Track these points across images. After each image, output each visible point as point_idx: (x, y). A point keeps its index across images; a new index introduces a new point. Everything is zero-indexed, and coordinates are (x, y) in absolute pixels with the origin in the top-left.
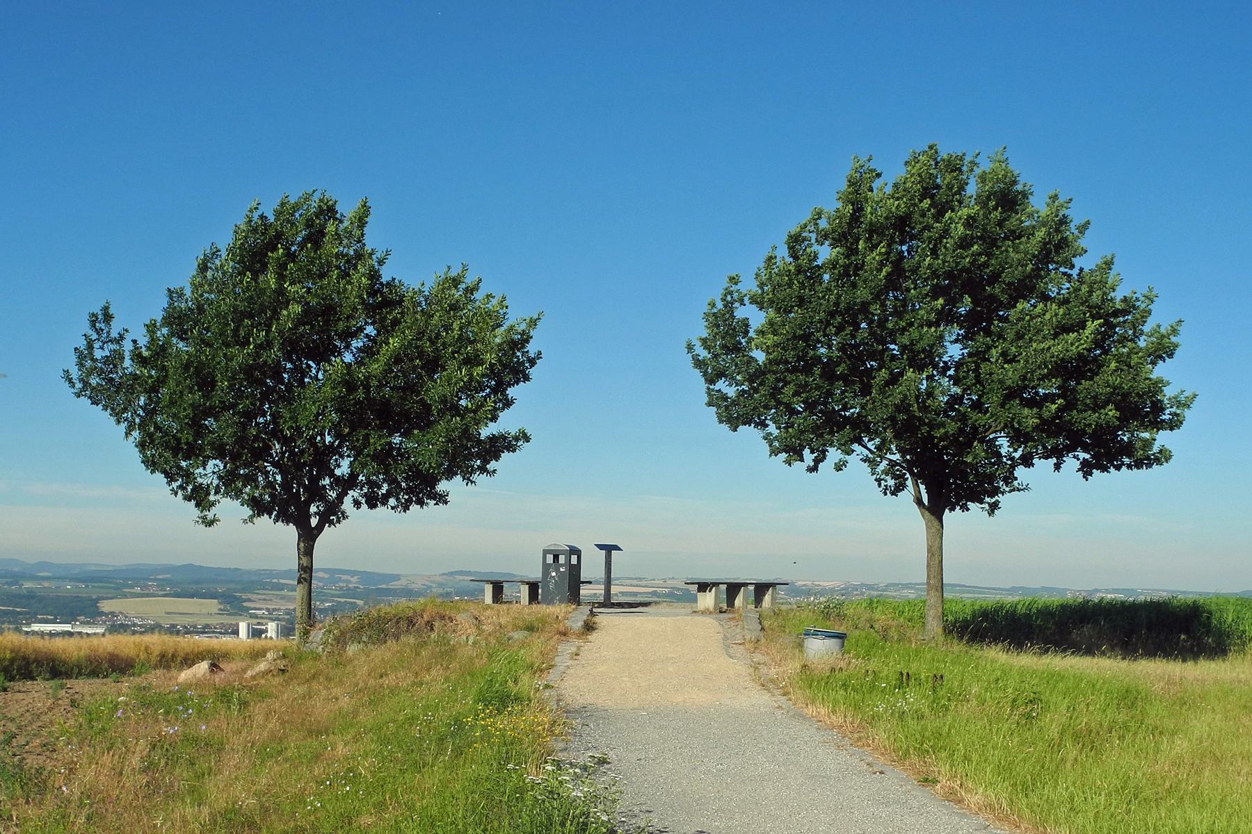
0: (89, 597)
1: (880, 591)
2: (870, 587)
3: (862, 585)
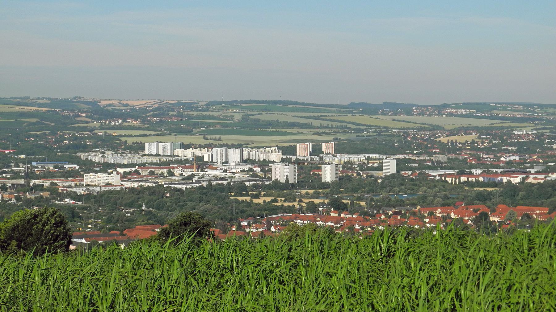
0: (103, 208)
1: (200, 110)
2: (189, 106)
3: (179, 104)
